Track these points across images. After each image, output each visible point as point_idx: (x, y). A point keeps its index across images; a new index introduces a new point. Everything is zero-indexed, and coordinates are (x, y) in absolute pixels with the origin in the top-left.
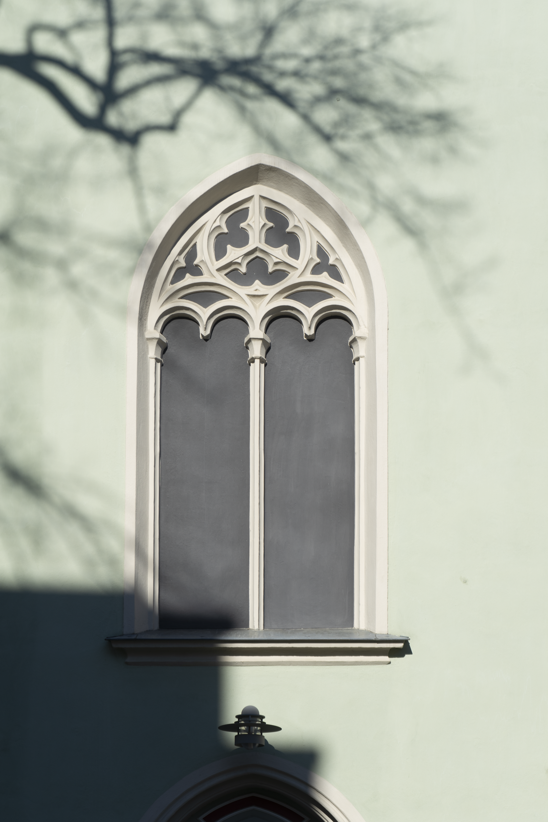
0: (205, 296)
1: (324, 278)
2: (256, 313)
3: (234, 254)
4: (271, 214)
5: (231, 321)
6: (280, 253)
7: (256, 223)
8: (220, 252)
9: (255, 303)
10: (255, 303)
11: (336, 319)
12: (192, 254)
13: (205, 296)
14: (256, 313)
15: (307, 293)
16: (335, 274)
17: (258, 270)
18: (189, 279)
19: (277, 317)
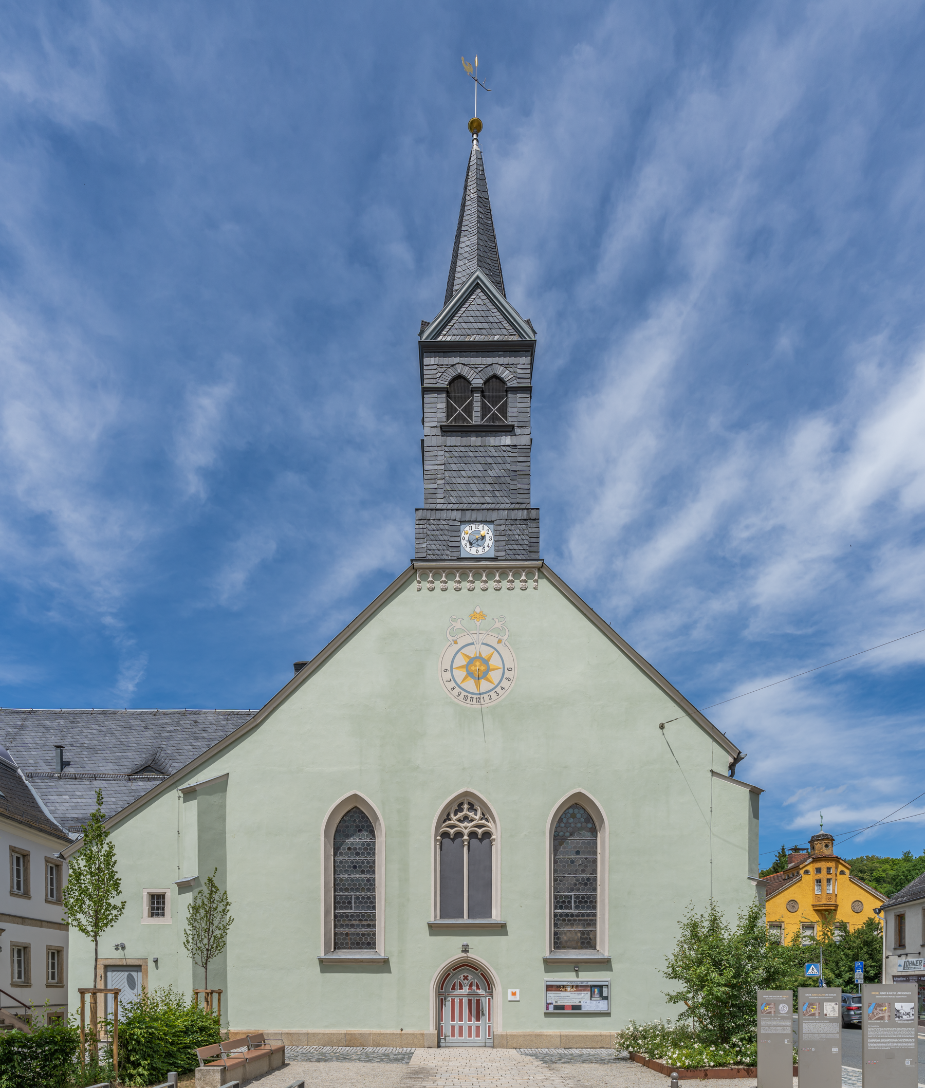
0: (452, 827)
1: (484, 821)
2: (466, 832)
3: (460, 815)
4: (469, 804)
5: (459, 834)
6: (471, 814)
7: (466, 806)
8: (456, 815)
9: (466, 828)
10: (466, 828)
11: (487, 835)
12: (448, 815)
13: (452, 827)
14: (466, 832)
15: (480, 826)
16: (487, 820)
17: (466, 818)
18: (448, 822)
19: (473, 835)
